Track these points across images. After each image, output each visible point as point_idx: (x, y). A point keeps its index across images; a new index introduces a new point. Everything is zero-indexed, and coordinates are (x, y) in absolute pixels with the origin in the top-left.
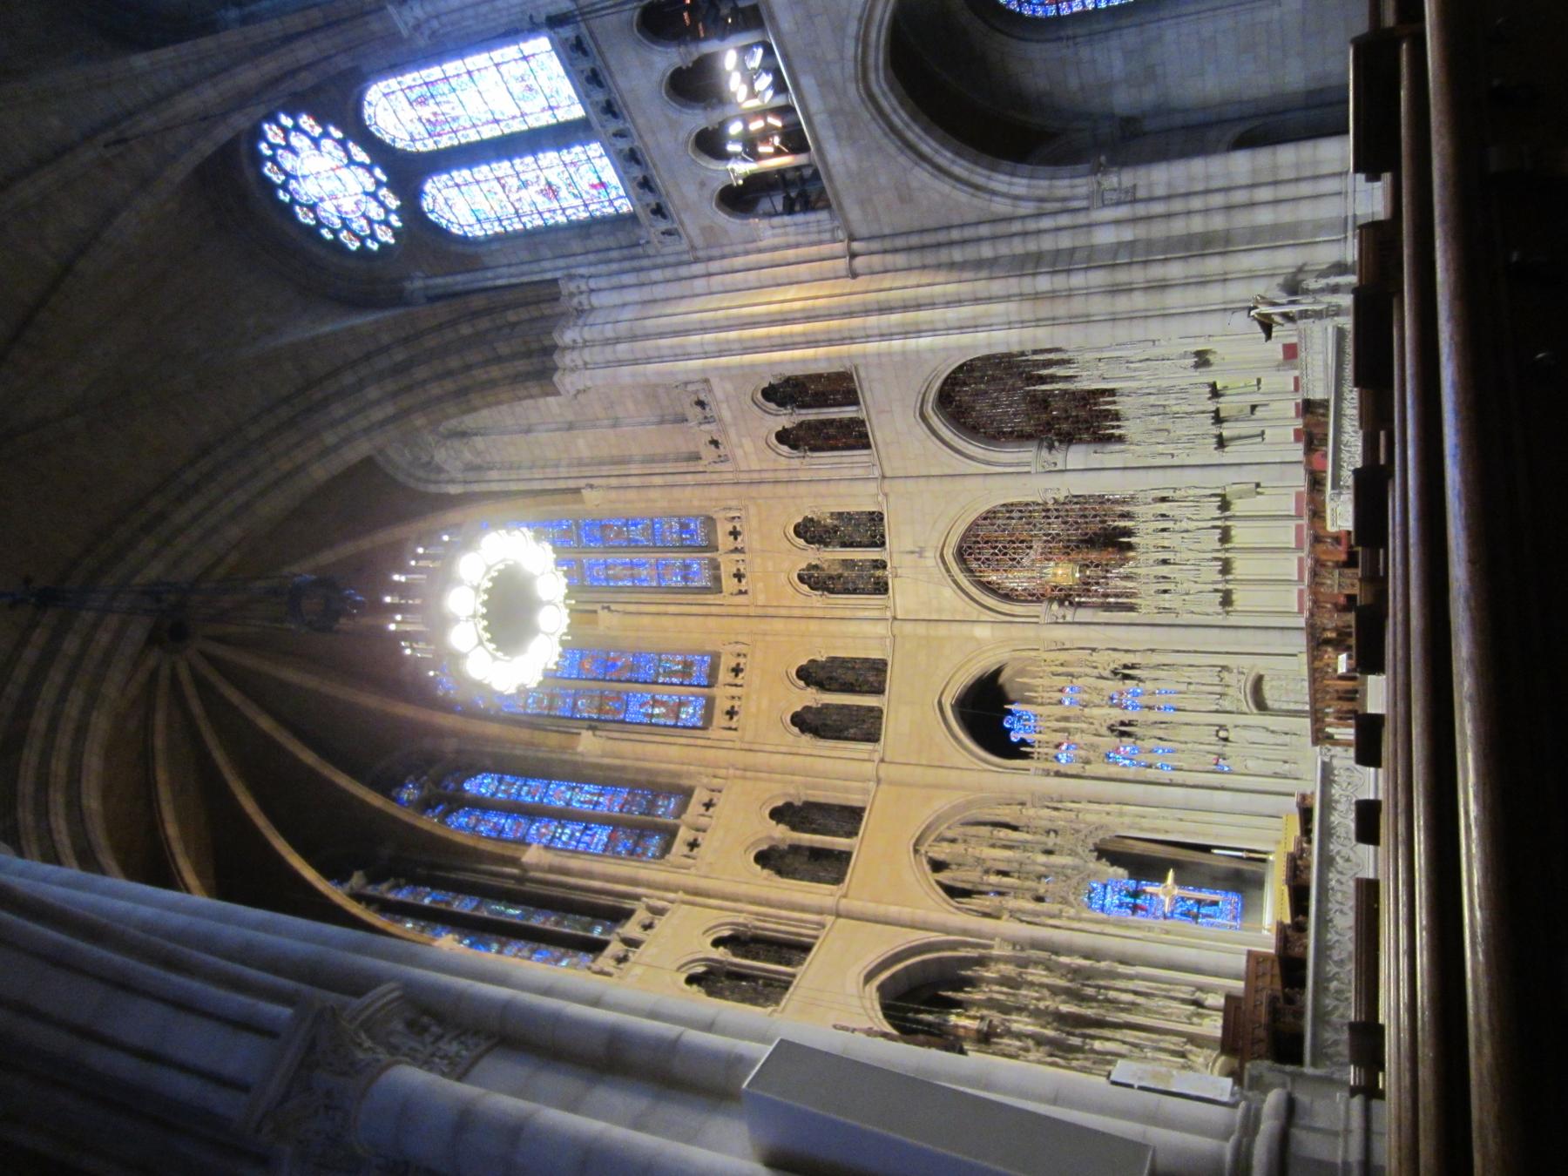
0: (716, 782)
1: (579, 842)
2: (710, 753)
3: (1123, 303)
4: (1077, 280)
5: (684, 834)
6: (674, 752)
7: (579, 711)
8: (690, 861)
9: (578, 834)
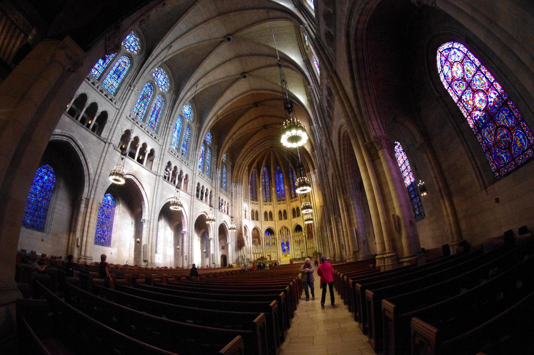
3: (318, 237)
4: (320, 233)
5: (280, 202)
6: (287, 197)
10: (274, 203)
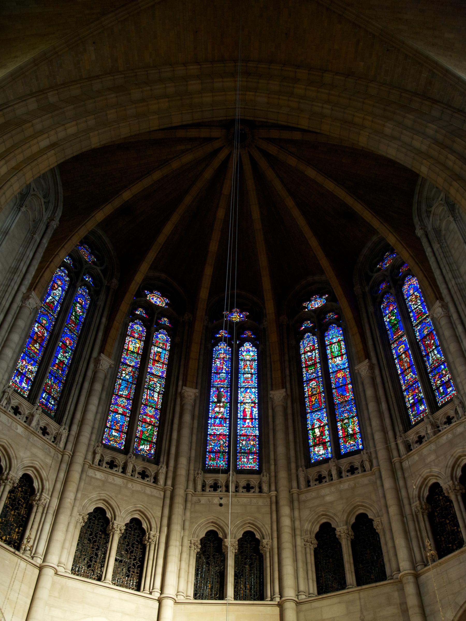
0: (265, 488)
1: (216, 418)
2: (283, 474)
7: (308, 385)
8: (199, 487)
9: (220, 416)
10: (182, 472)
